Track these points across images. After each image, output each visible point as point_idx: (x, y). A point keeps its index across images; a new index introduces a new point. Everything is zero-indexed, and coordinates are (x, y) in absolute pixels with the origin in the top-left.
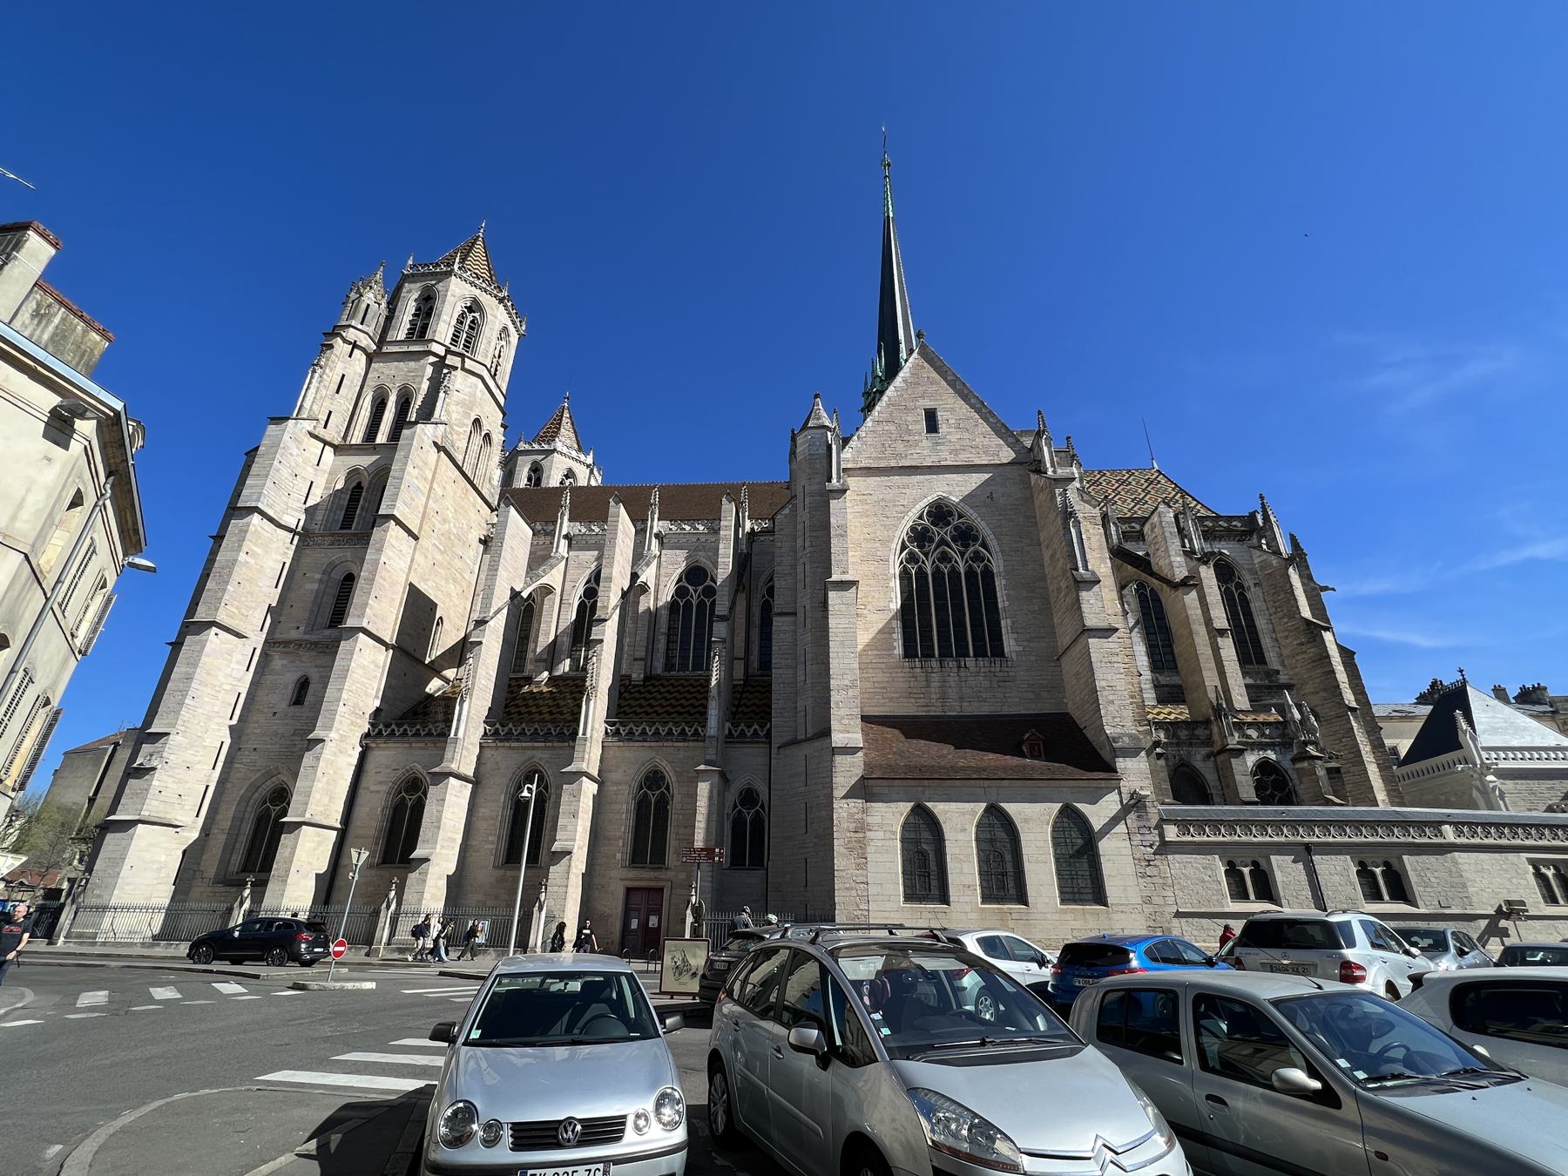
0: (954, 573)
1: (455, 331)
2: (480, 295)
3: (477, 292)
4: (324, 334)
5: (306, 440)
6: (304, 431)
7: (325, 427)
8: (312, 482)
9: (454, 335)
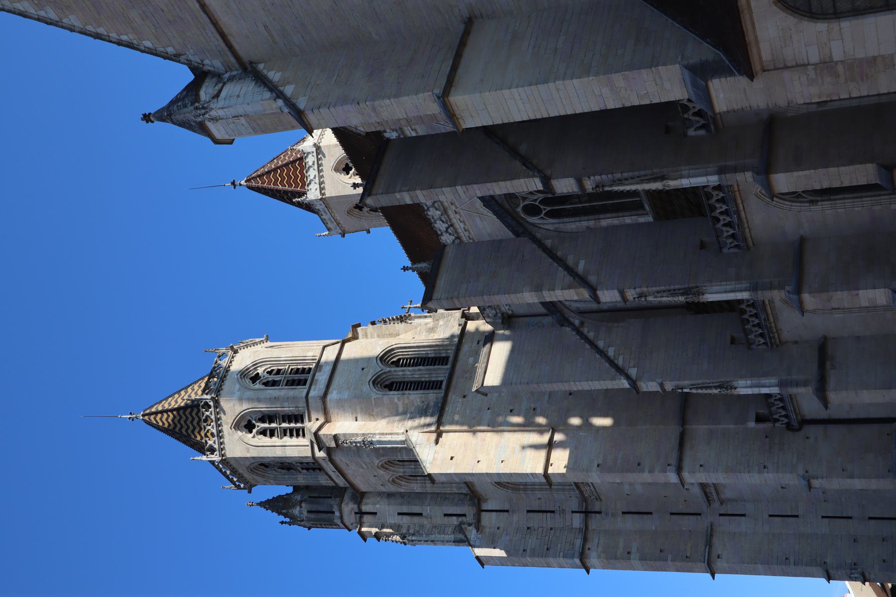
1: (285, 435)
2: (227, 424)
3: (226, 428)
4: (365, 540)
5: (487, 530)
6: (480, 536)
7: (464, 515)
8: (528, 511)
9: (291, 435)
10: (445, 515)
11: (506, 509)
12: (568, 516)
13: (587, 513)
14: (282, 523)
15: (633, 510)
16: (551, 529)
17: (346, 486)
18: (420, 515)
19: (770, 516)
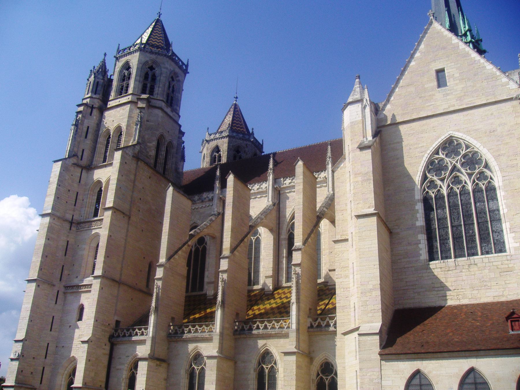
0: (464, 192)
3: (153, 57)
7: (81, 159)
8: (77, 193)
10: (83, 150)
11: (81, 181)
12: (72, 212)
13: (71, 223)
14: (94, 67)
15: (69, 247)
16: (67, 202)
17: (108, 105)
18: (86, 137)
19: (53, 317)
